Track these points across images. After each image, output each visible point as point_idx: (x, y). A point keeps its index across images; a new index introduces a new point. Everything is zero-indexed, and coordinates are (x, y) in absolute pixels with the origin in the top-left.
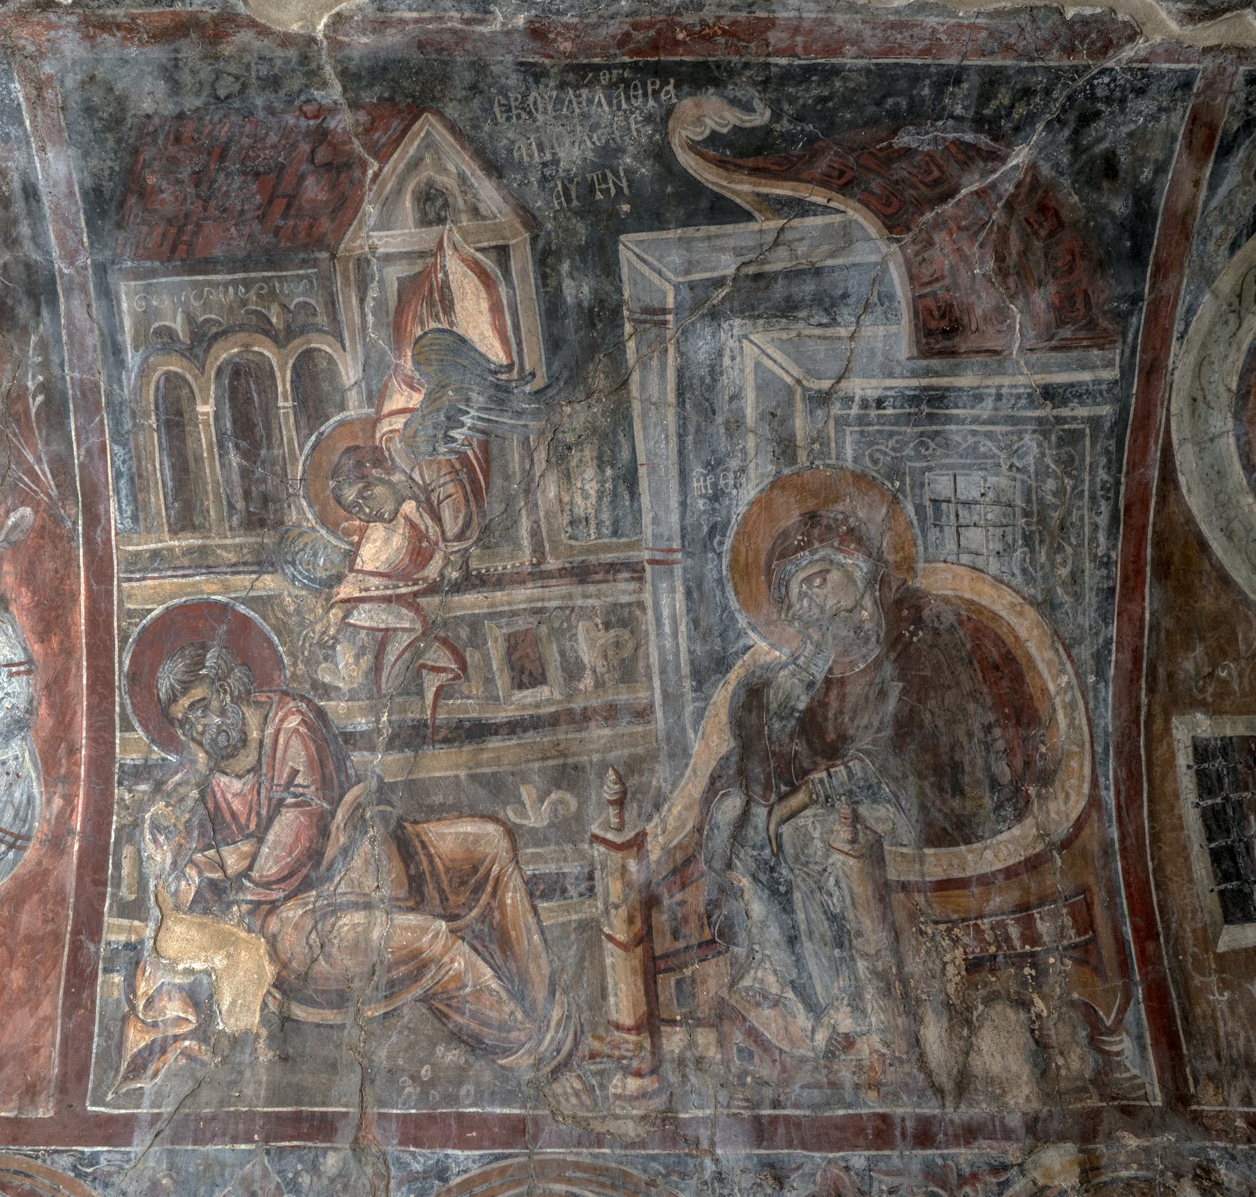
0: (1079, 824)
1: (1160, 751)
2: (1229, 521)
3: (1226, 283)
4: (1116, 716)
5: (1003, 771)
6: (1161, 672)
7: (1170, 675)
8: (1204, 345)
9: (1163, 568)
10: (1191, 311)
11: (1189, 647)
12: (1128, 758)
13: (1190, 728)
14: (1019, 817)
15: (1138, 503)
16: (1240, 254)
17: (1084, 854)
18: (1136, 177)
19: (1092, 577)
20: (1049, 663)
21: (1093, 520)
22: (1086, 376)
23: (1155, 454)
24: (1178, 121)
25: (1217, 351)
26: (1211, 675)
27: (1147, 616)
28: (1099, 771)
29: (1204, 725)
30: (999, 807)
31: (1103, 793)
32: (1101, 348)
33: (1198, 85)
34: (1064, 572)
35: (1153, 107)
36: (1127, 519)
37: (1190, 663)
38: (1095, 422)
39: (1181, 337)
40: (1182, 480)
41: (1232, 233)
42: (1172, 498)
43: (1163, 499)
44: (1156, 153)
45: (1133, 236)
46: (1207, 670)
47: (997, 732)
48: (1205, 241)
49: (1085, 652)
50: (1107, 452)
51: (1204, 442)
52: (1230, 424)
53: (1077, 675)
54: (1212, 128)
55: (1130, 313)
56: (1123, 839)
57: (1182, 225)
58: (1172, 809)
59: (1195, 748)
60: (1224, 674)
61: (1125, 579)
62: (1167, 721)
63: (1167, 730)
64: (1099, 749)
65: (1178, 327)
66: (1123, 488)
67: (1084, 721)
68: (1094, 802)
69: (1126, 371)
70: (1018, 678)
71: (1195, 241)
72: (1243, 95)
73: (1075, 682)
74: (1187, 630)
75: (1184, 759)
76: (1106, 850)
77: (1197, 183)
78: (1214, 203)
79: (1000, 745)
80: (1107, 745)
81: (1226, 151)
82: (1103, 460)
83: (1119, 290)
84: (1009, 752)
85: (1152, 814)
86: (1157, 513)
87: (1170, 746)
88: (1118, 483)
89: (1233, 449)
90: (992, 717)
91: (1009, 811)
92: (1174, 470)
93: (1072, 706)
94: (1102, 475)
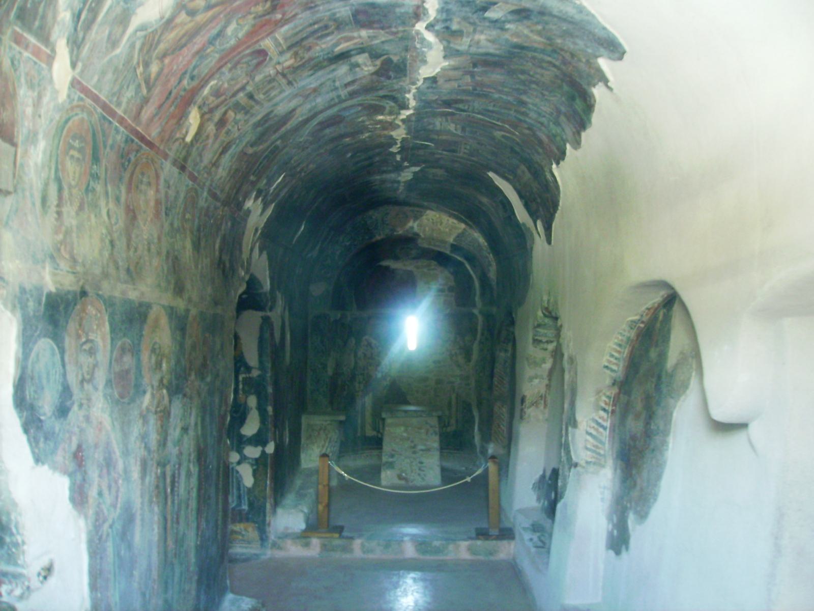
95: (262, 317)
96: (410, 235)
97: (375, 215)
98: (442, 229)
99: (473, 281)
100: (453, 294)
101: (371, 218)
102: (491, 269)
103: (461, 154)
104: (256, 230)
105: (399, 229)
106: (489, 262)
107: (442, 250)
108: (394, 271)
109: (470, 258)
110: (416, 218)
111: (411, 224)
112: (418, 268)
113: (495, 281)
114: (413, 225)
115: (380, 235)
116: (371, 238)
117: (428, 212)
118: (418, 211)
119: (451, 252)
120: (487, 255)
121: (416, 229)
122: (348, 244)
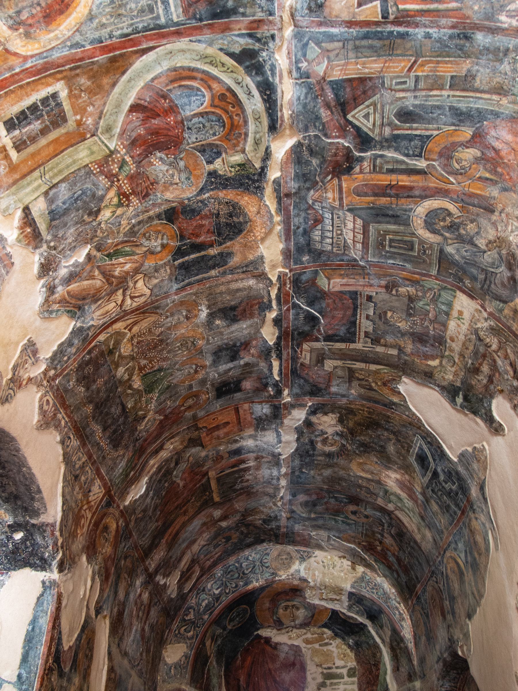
0: (15, 54)
1: (50, 80)
2: (134, 79)
3: (210, 51)
4: (58, 58)
5: (25, 15)
6: (78, 71)
7: (78, 75)
8: (189, 50)
9: (113, 60)
10: (199, 41)
11: (89, 79)
12: (46, 67)
13: (60, 88)
14: (10, 28)
15: (134, 43)
16: (219, 52)
17: (6, 59)
18: (240, 7)
19: (104, 33)
20: (70, 24)
21: (124, 27)
22: (173, 9)
23: (151, 44)
24: (260, 15)
25: (188, 55)
26: (82, 91)
27: (96, 59)
28: (37, 57)
29: (63, 94)
30: (11, 17)
31: (30, 61)
32: (183, 12)
33: (271, 18)
34: (104, 21)
35: (263, 5)
36: (128, 40)
37: (84, 81)
38: (158, 17)
39: (191, 41)
40: (144, 57)
41: (225, 47)
42: (137, 55)
43: (136, 52)
44: (248, 11)
45: (221, 12)
46: (83, 88)
47: (39, 9)
48: (222, 38)
49: (78, 38)
50: (149, 25)
51: (158, 62)
52: (165, 68)
53: (69, 37)
54: (257, 28)
55: (196, 19)
56: (17, 74)
57: (226, 29)
58: (33, 90)
59: (55, 93)
60: (83, 95)
61: (106, 46)
62: (62, 79)
63: (58, 80)
64: (45, 55)
65: (193, 38)
66: (137, 35)
67: (53, 45)
68: (26, 58)
69: (177, 24)
70: (61, 12)
71: (221, 35)
72: (268, 35)
73: (66, 37)
74: (94, 76)
75: (50, 90)
76: (11, 68)
77: (240, 29)
78: (234, 38)
79: (34, 11)
80: (46, 57)
81: (250, 36)
82: (146, 25)
83: (203, 12)
84: (33, 16)
85: (28, 83)
86: (132, 51)
87: (53, 83)
88: (139, 33)
89: (158, 72)
90: (43, 4)
91: (11, 22)
92: (147, 53)
93: (57, 38)
94: (141, 26)
95: (43, 582)
96: (296, 582)
97: (251, 555)
98: (335, 573)
99: (381, 652)
100: (355, 679)
101: (248, 559)
102: (403, 623)
103: (359, 346)
104: (31, 349)
105: (281, 573)
106: (400, 614)
107: (337, 607)
108: (276, 646)
109: (374, 614)
110: (303, 559)
111: (296, 566)
112: (307, 642)
113: (412, 641)
114: (299, 569)
115: (257, 580)
116: (246, 584)
117: (317, 553)
118: (304, 552)
119: (350, 608)
120: (397, 605)
121: (303, 574)
122: (217, 592)
